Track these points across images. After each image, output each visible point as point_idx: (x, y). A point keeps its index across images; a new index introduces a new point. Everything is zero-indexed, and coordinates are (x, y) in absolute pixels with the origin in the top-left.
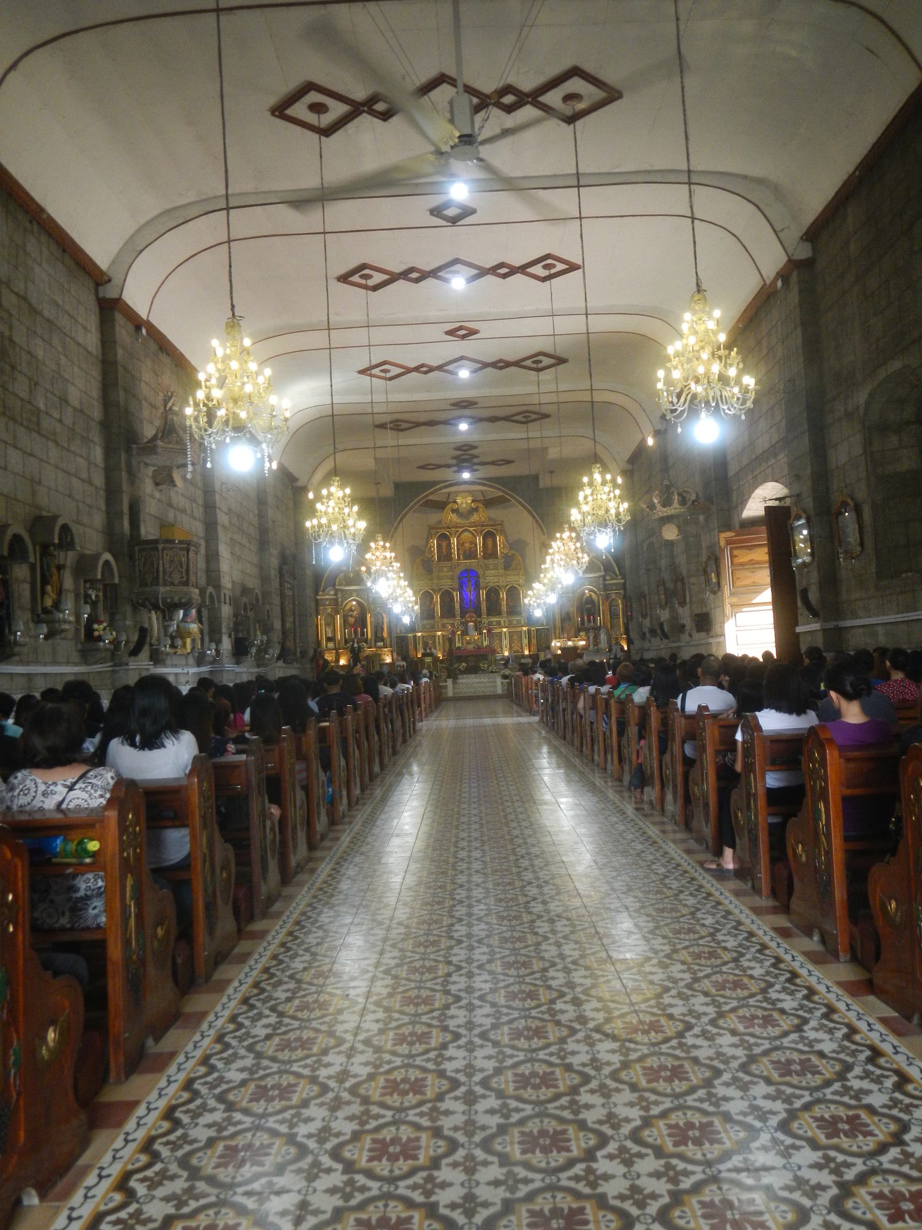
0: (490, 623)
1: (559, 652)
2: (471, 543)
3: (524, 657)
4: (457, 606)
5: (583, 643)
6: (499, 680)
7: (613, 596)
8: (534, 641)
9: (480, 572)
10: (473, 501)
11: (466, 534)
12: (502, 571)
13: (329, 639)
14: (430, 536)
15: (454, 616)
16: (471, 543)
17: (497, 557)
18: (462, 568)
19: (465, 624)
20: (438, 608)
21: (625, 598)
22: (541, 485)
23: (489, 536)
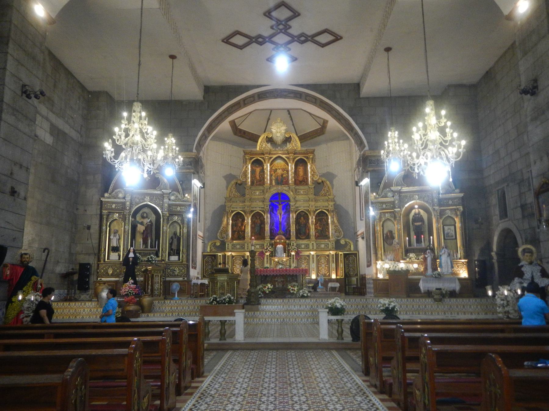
0: (298, 246)
1: (387, 277)
2: (283, 170)
3: (332, 280)
4: (267, 228)
5: (416, 266)
6: (324, 317)
7: (448, 213)
8: (341, 265)
9: (291, 195)
10: (286, 131)
11: (279, 162)
12: (312, 196)
13: (116, 249)
14: (245, 162)
15: (263, 238)
16: (283, 170)
17: (307, 184)
18: (274, 191)
19: (274, 245)
20: (248, 230)
21: (465, 217)
22: (367, 90)
23: (301, 163)
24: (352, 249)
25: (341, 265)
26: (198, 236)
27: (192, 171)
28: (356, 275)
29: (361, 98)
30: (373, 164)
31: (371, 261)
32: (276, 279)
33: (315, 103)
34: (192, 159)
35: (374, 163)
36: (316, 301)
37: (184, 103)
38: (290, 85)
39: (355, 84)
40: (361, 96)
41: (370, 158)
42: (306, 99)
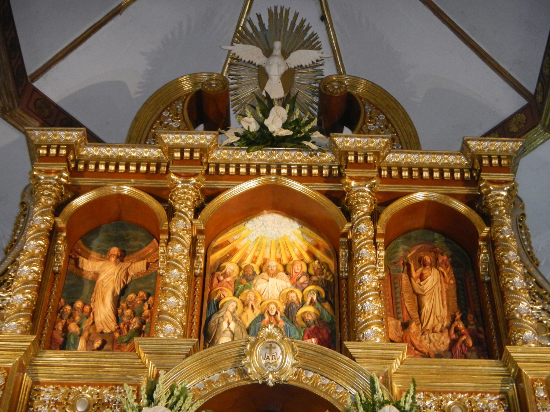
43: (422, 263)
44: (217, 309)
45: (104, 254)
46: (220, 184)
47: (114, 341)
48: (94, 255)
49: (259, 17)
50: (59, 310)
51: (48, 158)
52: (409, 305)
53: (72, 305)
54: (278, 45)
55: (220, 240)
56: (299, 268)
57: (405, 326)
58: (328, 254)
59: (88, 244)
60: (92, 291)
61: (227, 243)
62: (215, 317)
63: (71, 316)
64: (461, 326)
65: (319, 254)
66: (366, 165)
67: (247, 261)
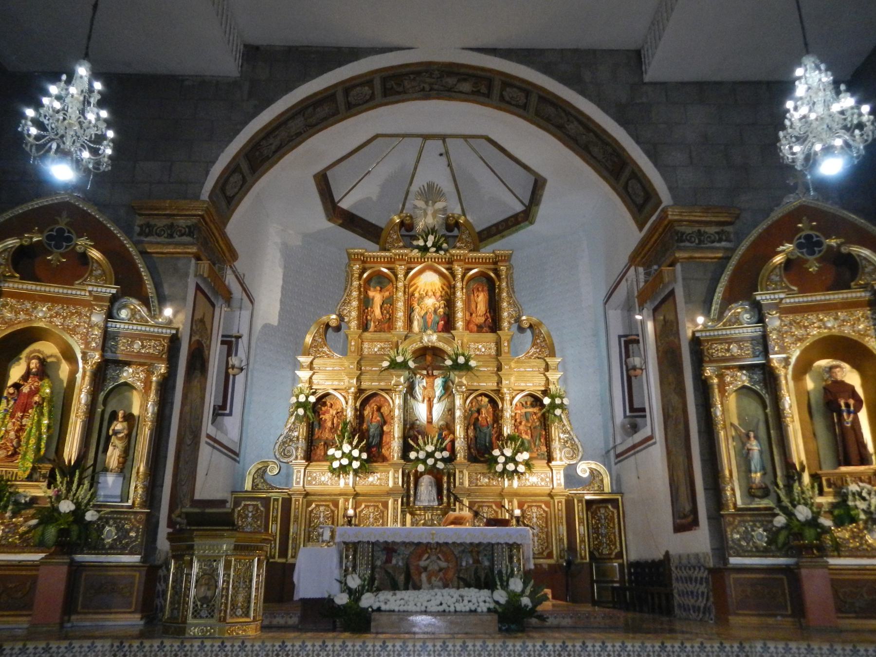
24: (607, 488)
25: (582, 527)
26: (204, 439)
27: (194, 250)
28: (620, 555)
29: (645, 84)
30: (687, 244)
31: (695, 511)
32: (422, 563)
33: (525, 107)
34: (194, 220)
35: (689, 241)
36: (564, 647)
37: (187, 83)
38: (463, 49)
39: (628, 51)
40: (647, 78)
41: (678, 228)
42: (502, 98)
43: (478, 290)
44: (413, 311)
45: (375, 290)
46: (412, 266)
47: (382, 322)
48: (372, 289)
49: (423, 186)
50: (364, 311)
51: (355, 260)
52: (473, 306)
53: (367, 308)
54: (430, 202)
55: (412, 283)
56: (439, 294)
57: (471, 314)
58: (447, 287)
59: (369, 285)
60: (373, 303)
61: (415, 284)
62: (412, 314)
63: (367, 313)
64: (488, 315)
65: (445, 287)
66: (460, 260)
67: (422, 292)
